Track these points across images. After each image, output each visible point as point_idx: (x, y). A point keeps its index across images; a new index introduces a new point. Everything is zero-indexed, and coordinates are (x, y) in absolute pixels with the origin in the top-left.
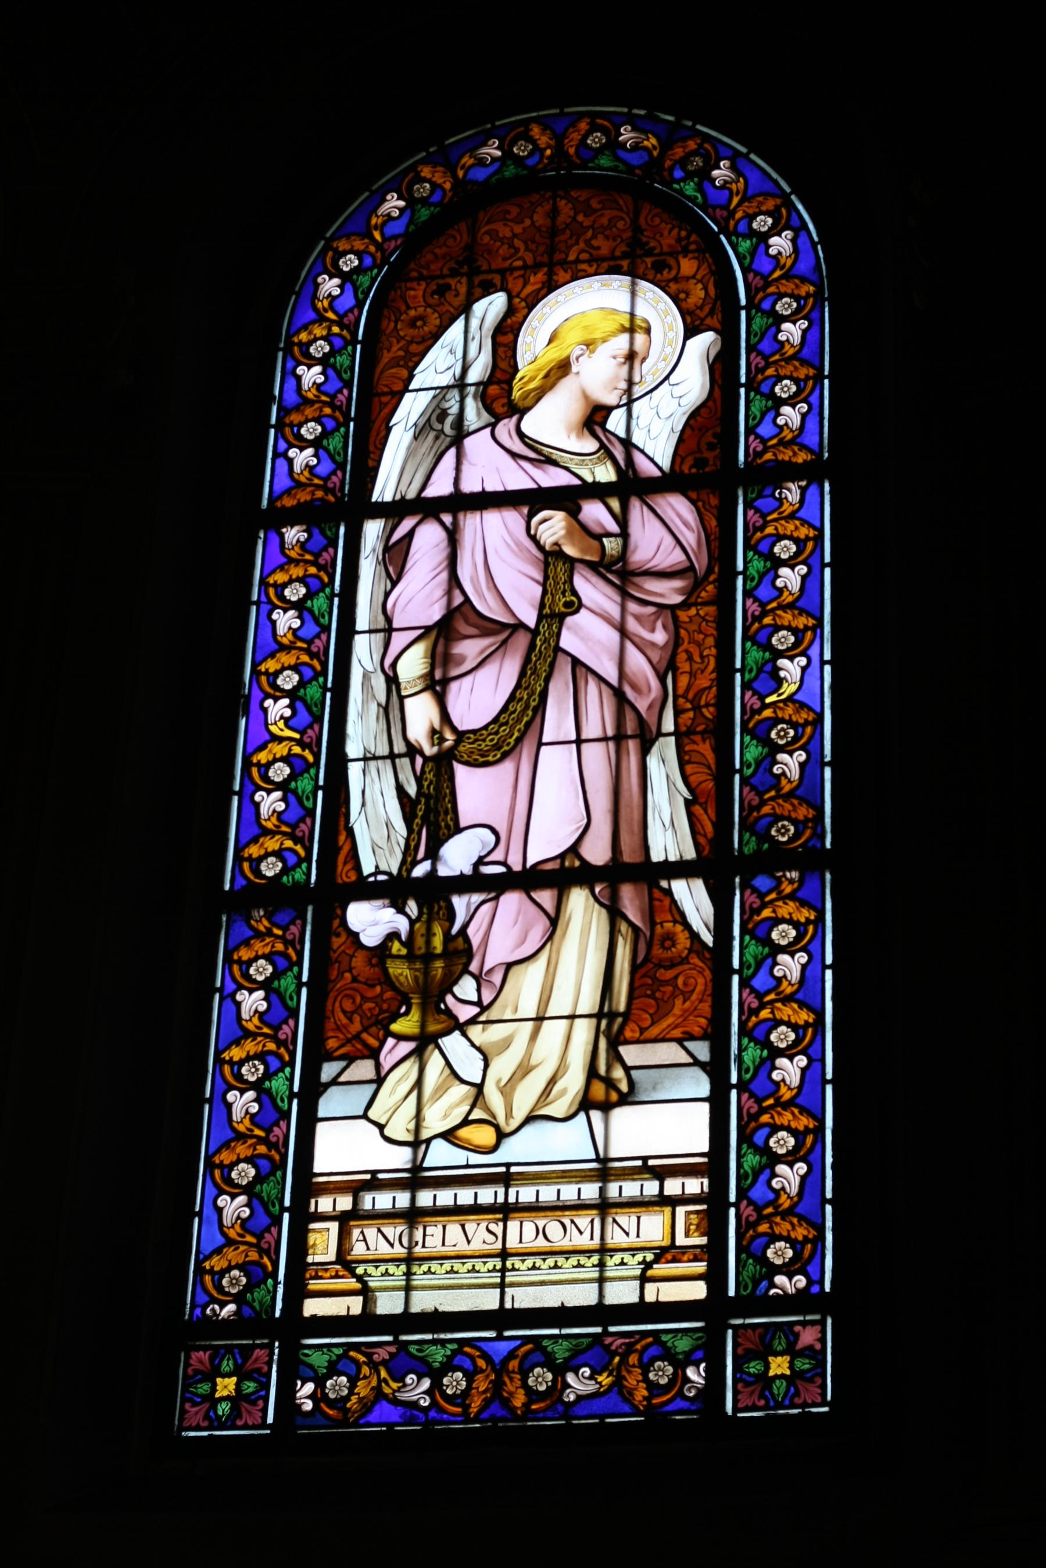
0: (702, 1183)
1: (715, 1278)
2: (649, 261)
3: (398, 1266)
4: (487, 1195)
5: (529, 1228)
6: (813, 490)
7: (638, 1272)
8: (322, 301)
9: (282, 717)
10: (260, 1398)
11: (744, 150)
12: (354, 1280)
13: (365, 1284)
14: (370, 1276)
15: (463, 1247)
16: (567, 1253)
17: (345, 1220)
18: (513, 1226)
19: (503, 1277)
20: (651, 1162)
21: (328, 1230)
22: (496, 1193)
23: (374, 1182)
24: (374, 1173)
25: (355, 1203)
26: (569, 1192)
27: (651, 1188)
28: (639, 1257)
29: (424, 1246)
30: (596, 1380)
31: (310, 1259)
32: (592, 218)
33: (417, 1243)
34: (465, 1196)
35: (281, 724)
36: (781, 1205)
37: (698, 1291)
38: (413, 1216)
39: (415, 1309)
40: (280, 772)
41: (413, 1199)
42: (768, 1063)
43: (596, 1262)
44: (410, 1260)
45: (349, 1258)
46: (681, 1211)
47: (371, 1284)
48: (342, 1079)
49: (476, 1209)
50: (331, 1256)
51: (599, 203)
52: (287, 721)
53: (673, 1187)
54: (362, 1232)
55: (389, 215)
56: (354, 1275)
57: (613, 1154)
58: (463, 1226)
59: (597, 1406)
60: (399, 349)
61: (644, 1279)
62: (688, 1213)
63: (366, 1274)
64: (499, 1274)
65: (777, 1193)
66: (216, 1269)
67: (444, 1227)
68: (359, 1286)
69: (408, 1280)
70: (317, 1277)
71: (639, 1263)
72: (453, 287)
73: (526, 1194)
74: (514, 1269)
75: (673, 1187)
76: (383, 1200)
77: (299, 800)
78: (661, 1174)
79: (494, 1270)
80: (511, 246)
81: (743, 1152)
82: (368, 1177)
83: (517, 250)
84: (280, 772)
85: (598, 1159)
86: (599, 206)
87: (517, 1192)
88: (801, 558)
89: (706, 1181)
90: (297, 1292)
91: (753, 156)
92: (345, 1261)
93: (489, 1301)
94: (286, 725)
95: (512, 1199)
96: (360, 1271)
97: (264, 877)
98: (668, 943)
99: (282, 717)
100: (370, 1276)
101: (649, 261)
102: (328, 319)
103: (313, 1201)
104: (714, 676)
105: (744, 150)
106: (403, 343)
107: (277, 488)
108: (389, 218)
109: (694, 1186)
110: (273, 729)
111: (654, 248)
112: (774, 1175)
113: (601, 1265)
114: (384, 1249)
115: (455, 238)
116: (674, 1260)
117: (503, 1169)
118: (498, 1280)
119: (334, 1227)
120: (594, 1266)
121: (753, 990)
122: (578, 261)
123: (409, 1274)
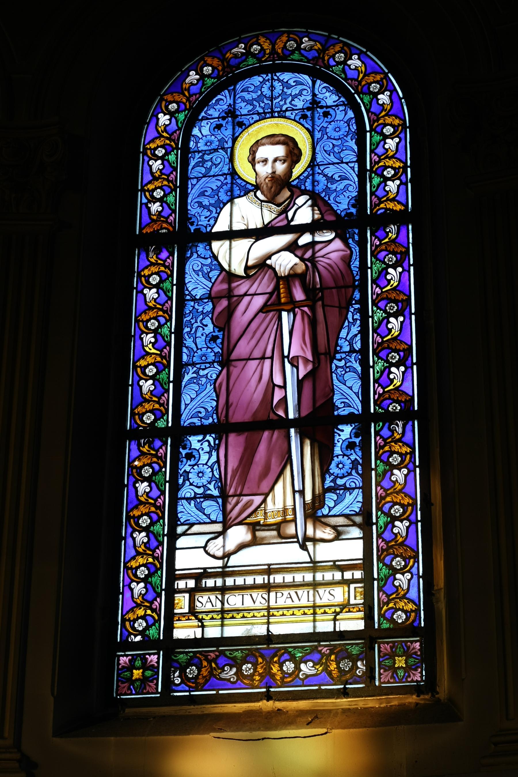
0: (362, 573)
1: (368, 618)
4: (260, 580)
6: (409, 427)
7: (332, 617)
8: (161, 127)
9: (150, 342)
10: (155, 679)
11: (365, 50)
12: (197, 621)
13: (202, 623)
14: (204, 619)
17: (192, 592)
18: (272, 595)
19: (268, 619)
20: (337, 563)
22: (264, 578)
23: (205, 574)
24: (205, 569)
26: (299, 578)
27: (338, 576)
28: (333, 610)
30: (315, 668)
31: (176, 611)
34: (249, 580)
35: (150, 346)
36: (398, 540)
37: (360, 625)
38: (224, 590)
39: (226, 635)
40: (151, 370)
41: (225, 582)
42: (392, 577)
43: (312, 612)
46: (352, 586)
47: (205, 624)
49: (254, 587)
50: (186, 610)
52: (153, 344)
53: (348, 575)
55: (191, 83)
57: (318, 559)
59: (315, 680)
61: (335, 620)
62: (355, 588)
63: (203, 619)
64: (267, 618)
65: (396, 535)
66: (132, 619)
68: (200, 624)
70: (179, 620)
71: (333, 613)
72: (224, 125)
73: (278, 578)
74: (273, 615)
75: (348, 575)
76: (210, 583)
77: (162, 385)
78: (342, 569)
79: (264, 616)
80: (253, 105)
81: (381, 622)
82: (202, 571)
84: (151, 370)
85: (312, 562)
87: (274, 578)
88: (405, 516)
90: (169, 628)
91: (368, 53)
92: (193, 612)
94: (153, 346)
95: (272, 581)
97: (146, 423)
99: (150, 342)
100: (204, 619)
102: (163, 137)
104: (359, 329)
105: (365, 50)
106: (201, 154)
107: (144, 224)
108: (192, 84)
109: (358, 574)
110: (147, 349)
112: (395, 579)
113: (315, 613)
116: (349, 611)
117: (266, 567)
119: (187, 595)
120: (311, 614)
121: (381, 437)
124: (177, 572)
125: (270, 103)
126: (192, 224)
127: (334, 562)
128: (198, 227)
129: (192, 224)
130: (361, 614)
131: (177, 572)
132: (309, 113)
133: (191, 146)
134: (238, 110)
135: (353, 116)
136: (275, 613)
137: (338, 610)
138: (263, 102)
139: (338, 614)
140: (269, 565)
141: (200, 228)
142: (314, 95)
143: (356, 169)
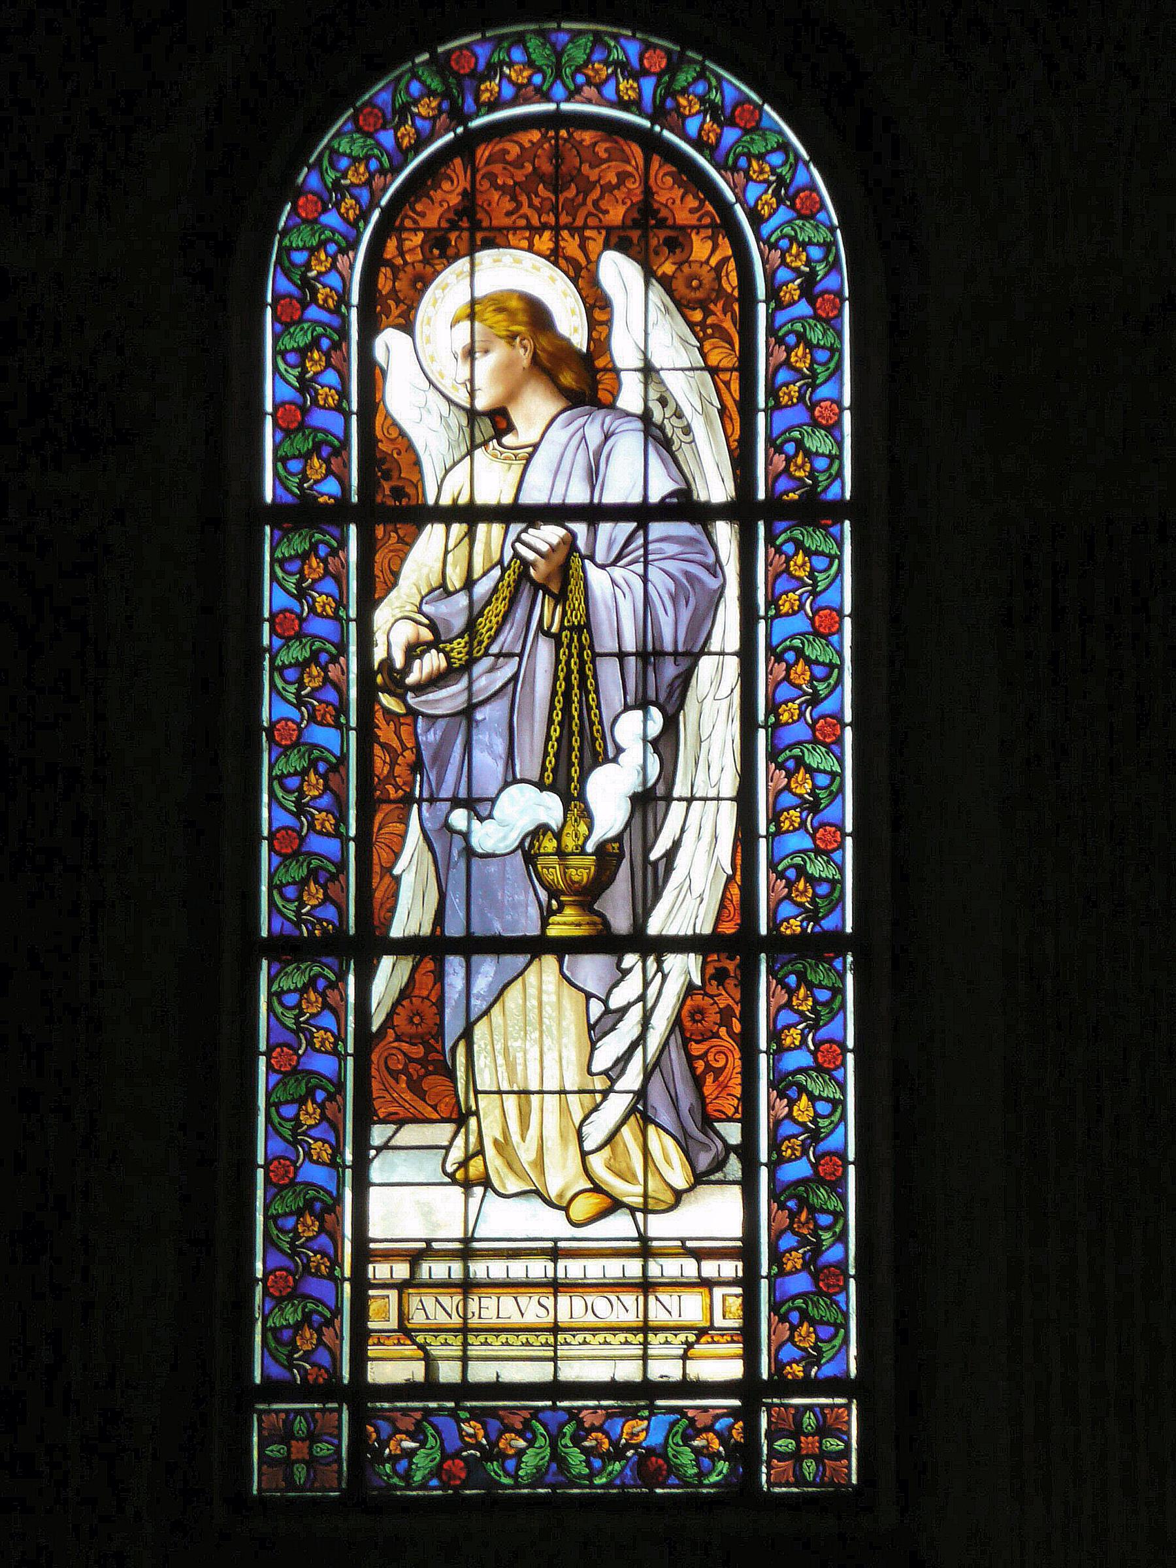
2: (663, 234)
3: (456, 1336)
5: (578, 1302)
15: (516, 1319)
16: (614, 1330)
20: (689, 1244)
21: (388, 1297)
25: (413, 1271)
29: (480, 1317)
32: (597, 171)
33: (473, 1313)
37: (734, 1370)
44: (465, 1330)
45: (409, 1326)
46: (718, 1292)
48: (393, 1143)
51: (606, 150)
53: (710, 1269)
54: (421, 1301)
56: (414, 1343)
58: (516, 1299)
60: (399, 316)
67: (499, 1298)
69: (465, 1351)
70: (379, 1344)
73: (573, 1269)
76: (438, 1270)
83: (519, 205)
86: (604, 155)
89: (740, 1264)
93: (540, 1373)
96: (420, 1339)
98: (698, 1017)
101: (663, 234)
103: (371, 1267)
111: (665, 219)
114: (442, 1319)
115: (452, 182)
118: (552, 1354)
122: (586, 226)
123: (465, 1344)
124: (372, 1246)
125: (553, 198)
126: (387, 476)
127: (683, 1240)
128: (400, 484)
129: (387, 476)
130: (737, 1348)
131: (372, 1246)
132: (635, 235)
133: (380, 287)
134: (482, 207)
135: (730, 252)
136: (569, 1339)
137: (692, 1338)
138: (537, 195)
139: (689, 1345)
140: (555, 1240)
141: (403, 488)
142: (648, 192)
143: (735, 386)
